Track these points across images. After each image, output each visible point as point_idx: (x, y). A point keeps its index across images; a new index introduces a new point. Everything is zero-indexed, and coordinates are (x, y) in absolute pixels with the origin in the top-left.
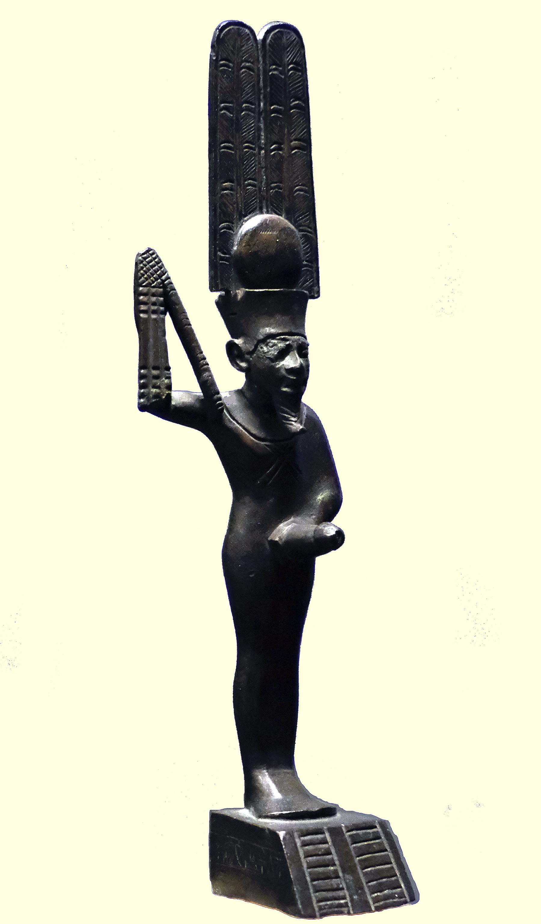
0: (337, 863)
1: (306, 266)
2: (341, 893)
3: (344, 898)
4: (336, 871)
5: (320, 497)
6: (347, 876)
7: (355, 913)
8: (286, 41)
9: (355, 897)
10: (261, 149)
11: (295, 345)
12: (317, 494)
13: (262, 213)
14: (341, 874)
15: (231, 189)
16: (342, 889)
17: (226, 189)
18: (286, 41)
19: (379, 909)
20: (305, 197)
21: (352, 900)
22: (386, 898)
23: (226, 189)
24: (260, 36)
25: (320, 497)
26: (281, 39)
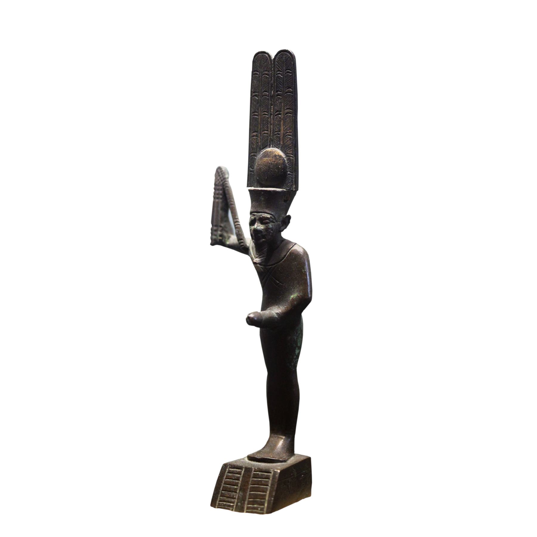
0: (239, 485)
1: (289, 174)
2: (233, 500)
3: (233, 503)
4: (236, 489)
5: (292, 296)
6: (241, 493)
7: (235, 511)
8: (286, 59)
9: (239, 504)
10: (271, 114)
11: (257, 218)
12: (292, 294)
13: (270, 147)
14: (238, 491)
15: (256, 136)
16: (235, 498)
17: (254, 136)
18: (286, 59)
19: (247, 512)
20: (290, 139)
21: (237, 505)
22: (254, 508)
23: (254, 136)
24: (273, 57)
25: (292, 296)
26: (282, 58)
